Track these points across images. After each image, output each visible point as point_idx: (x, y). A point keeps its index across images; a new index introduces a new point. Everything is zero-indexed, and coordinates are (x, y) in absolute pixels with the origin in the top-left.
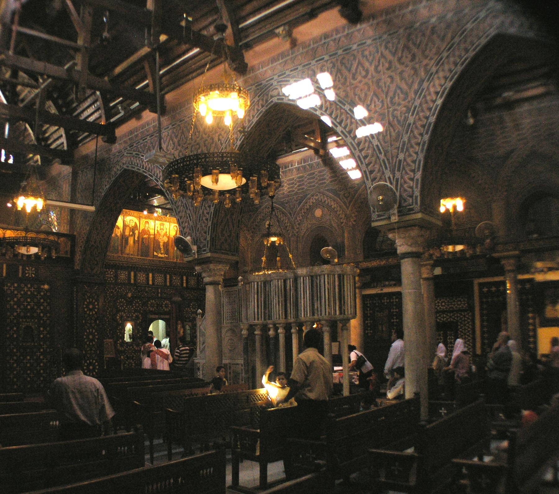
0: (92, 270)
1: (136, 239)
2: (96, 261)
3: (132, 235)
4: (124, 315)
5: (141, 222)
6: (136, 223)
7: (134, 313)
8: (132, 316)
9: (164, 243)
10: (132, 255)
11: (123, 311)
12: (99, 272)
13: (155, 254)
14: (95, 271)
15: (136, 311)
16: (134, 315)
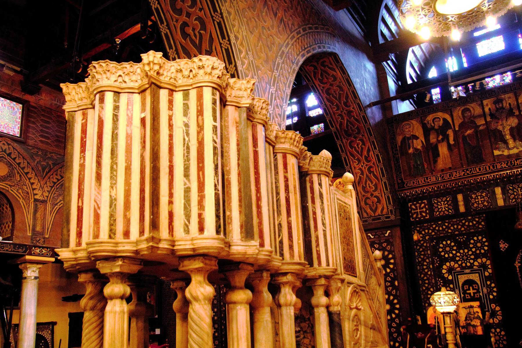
0: (374, 211)
1: (452, 142)
2: (376, 197)
3: (443, 140)
4: (456, 266)
5: (455, 114)
6: (445, 120)
7: (475, 260)
8: (472, 265)
9: (511, 129)
10: (450, 168)
11: (453, 259)
12: (385, 210)
13: (496, 153)
14: (379, 211)
15: (477, 257)
16: (476, 263)
